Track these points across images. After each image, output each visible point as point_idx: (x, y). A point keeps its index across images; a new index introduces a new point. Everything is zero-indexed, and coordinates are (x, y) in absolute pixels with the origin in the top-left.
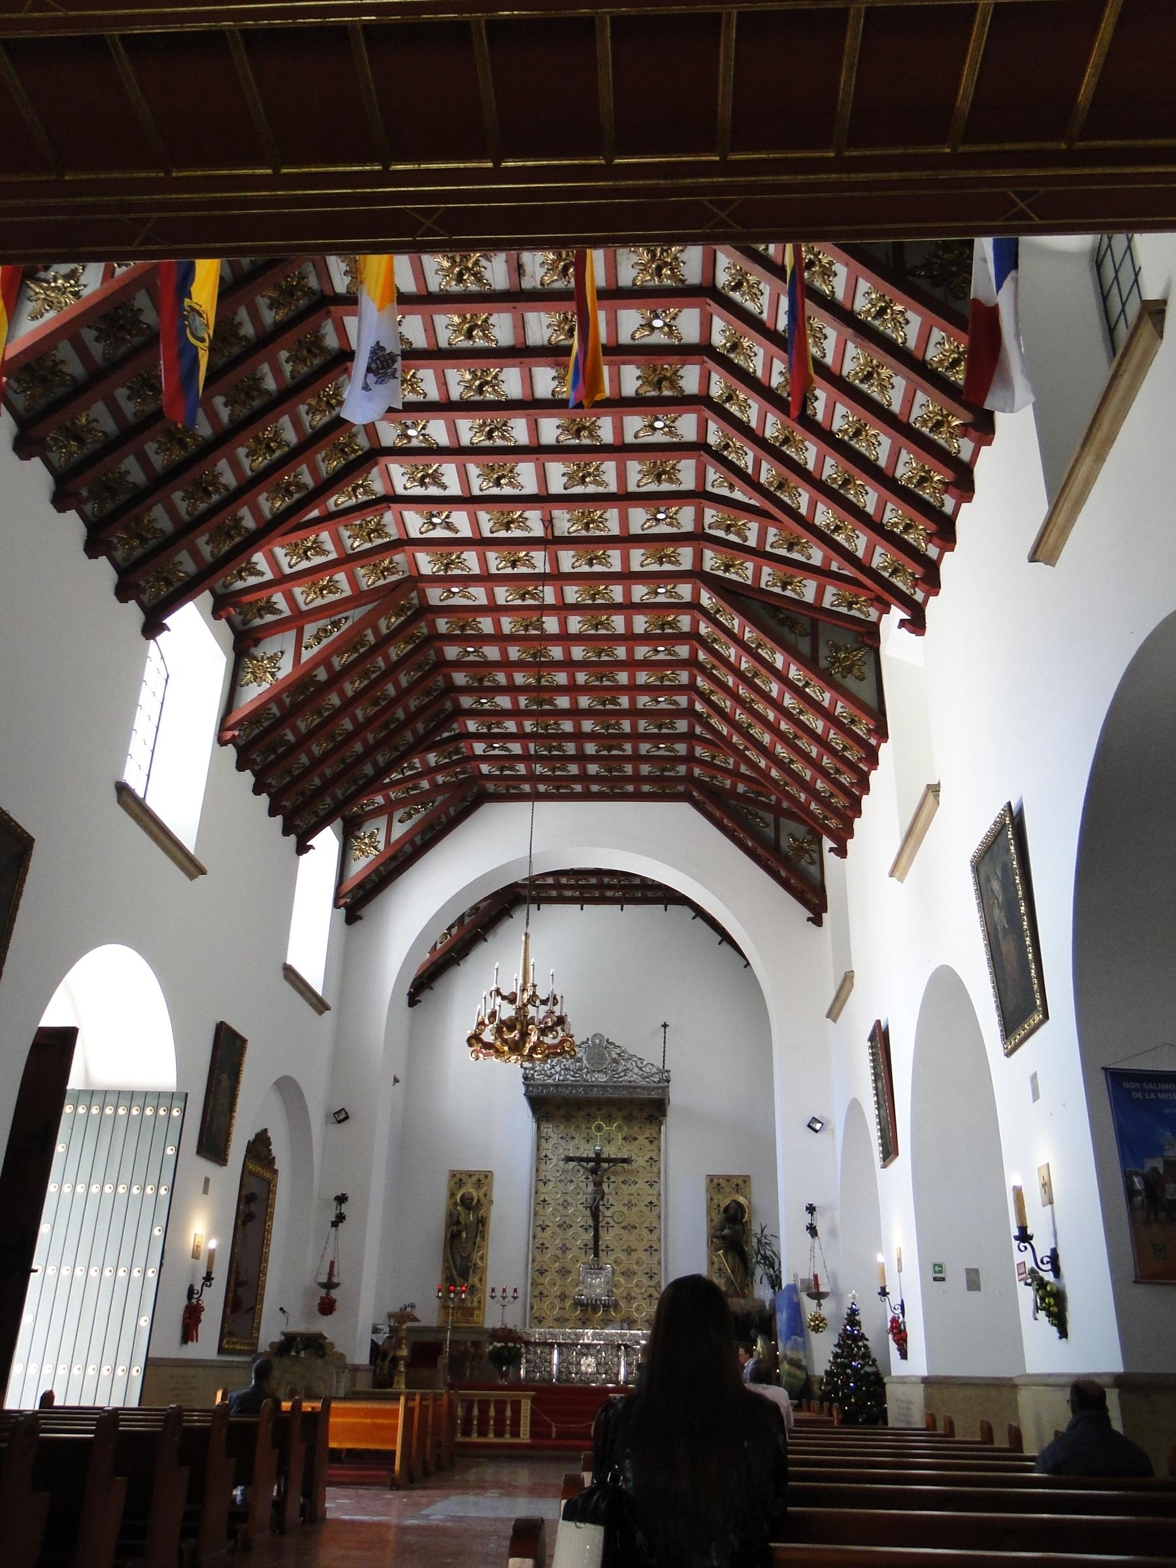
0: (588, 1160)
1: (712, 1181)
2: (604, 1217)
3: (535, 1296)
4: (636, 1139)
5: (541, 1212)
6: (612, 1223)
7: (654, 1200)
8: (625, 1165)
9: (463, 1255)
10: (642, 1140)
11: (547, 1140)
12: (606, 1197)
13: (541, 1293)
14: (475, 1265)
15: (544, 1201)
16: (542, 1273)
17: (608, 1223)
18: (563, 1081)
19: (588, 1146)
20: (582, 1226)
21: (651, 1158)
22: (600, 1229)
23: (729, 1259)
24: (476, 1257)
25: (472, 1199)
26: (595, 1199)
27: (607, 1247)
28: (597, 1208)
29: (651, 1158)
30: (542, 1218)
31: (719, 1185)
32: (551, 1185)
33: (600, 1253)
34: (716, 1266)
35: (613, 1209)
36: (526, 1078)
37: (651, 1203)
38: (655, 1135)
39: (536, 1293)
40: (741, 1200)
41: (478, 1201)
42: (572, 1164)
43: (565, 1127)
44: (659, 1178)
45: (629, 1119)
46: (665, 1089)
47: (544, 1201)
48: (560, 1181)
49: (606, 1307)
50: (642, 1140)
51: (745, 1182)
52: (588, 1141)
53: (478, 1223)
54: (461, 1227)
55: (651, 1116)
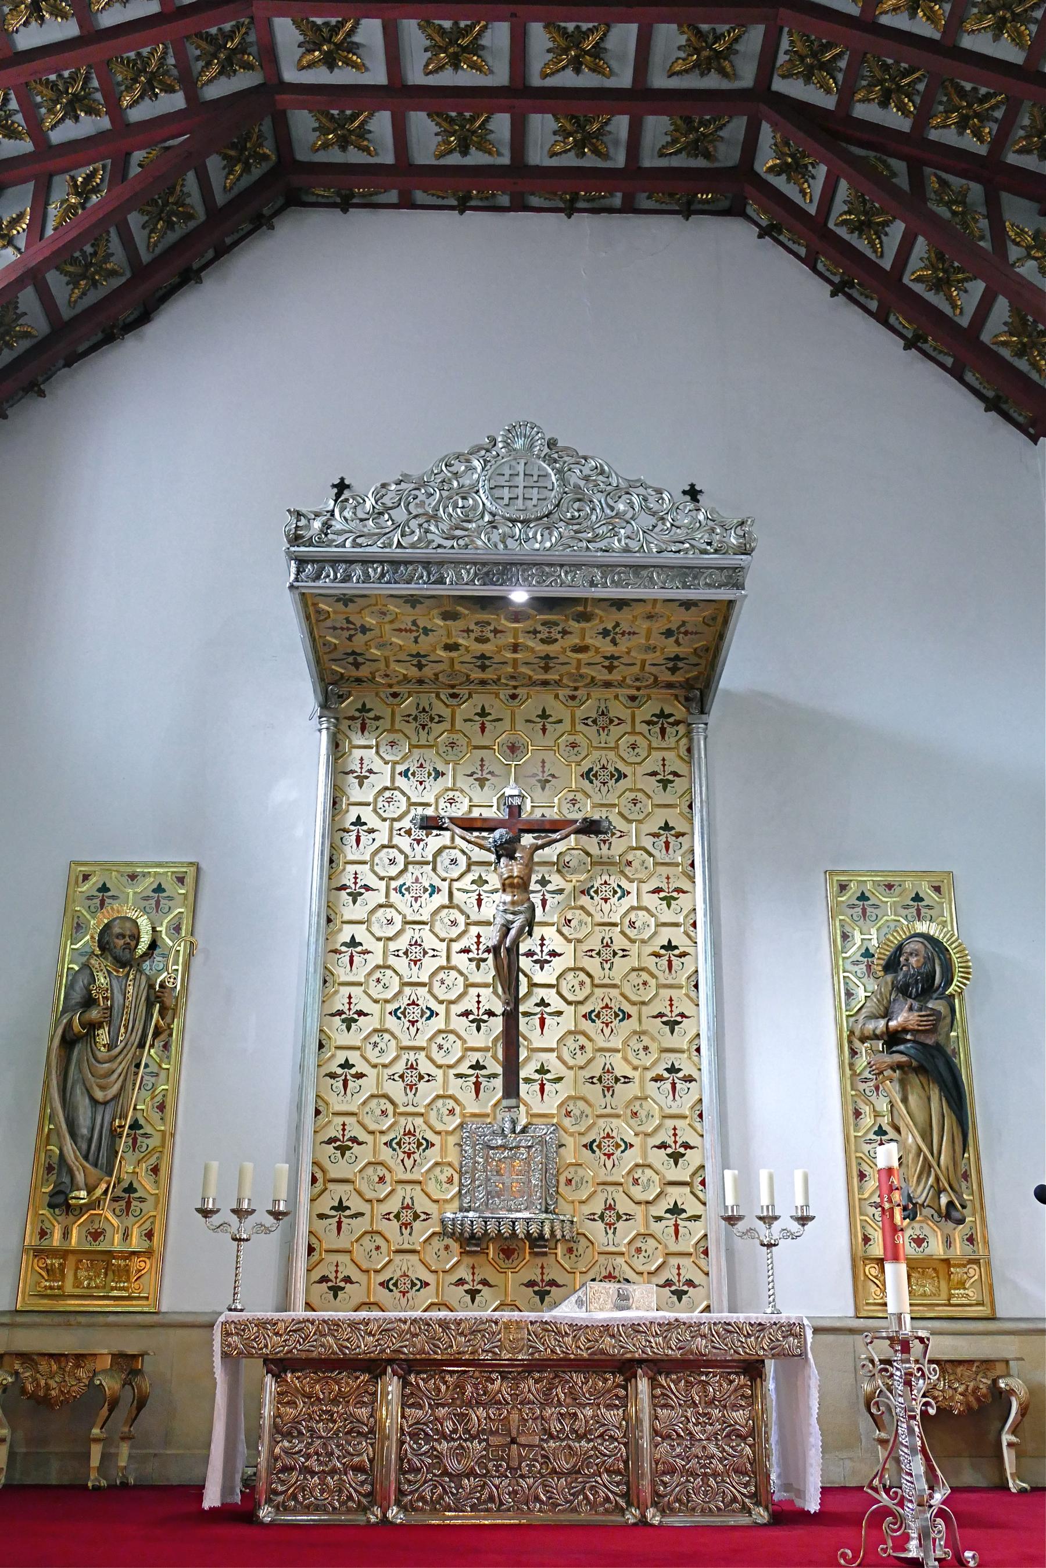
0: (487, 825)
1: (843, 887)
2: (532, 985)
3: (322, 1216)
4: (621, 776)
5: (343, 974)
6: (556, 1003)
7: (677, 937)
8: (590, 842)
9: (99, 1095)
10: (638, 778)
11: (361, 780)
12: (538, 931)
13: (341, 1207)
14: (135, 1126)
15: (353, 943)
16: (343, 1150)
17: (542, 1003)
18: (413, 546)
19: (479, 795)
20: (466, 1014)
21: (667, 827)
22: (522, 1020)
23: (910, 1098)
24: (141, 1103)
25: (136, 938)
26: (506, 928)
27: (542, 1071)
28: (513, 951)
29: (667, 827)
30: (345, 991)
31: (863, 897)
32: (373, 899)
33: (523, 1088)
34: (867, 1121)
35: (558, 965)
36: (296, 539)
37: (669, 947)
38: (675, 764)
39: (325, 1205)
40: (932, 929)
41: (153, 945)
42: (435, 841)
43: (412, 747)
44: (692, 879)
45: (603, 720)
46: (734, 578)
47: (353, 943)
48: (399, 890)
49: (538, 1243)
50: (638, 778)
51: (937, 889)
52: (482, 782)
53: (150, 1006)
54: (94, 1014)
55: (662, 715)
